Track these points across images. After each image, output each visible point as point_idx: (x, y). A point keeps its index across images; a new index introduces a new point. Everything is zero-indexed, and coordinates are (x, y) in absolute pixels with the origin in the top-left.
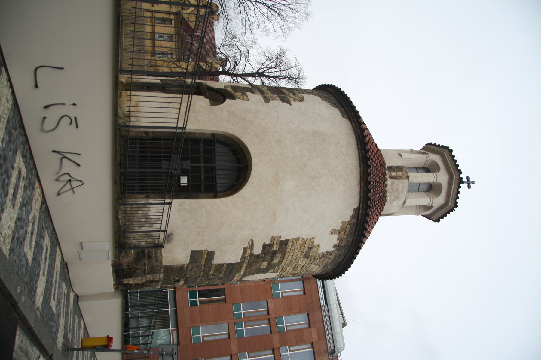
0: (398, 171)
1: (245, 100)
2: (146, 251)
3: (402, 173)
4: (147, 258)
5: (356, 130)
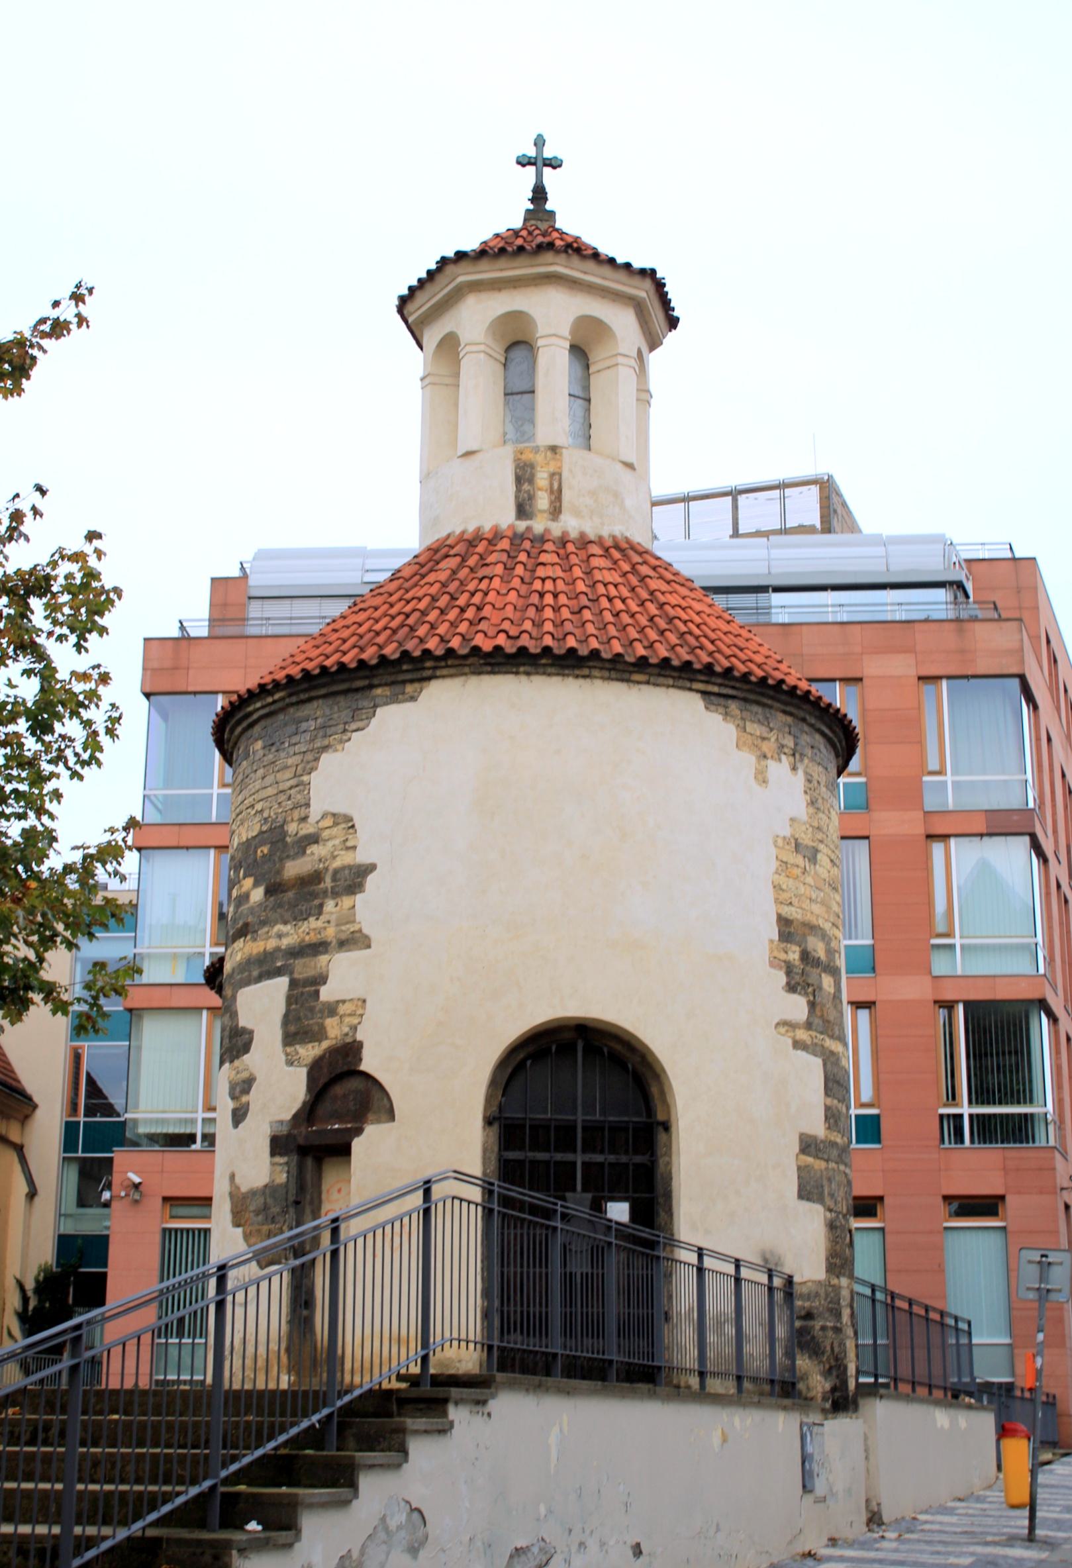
0: (531, 481)
1: (360, 1012)
2: (798, 1324)
3: (539, 469)
4: (811, 1323)
5: (467, 670)
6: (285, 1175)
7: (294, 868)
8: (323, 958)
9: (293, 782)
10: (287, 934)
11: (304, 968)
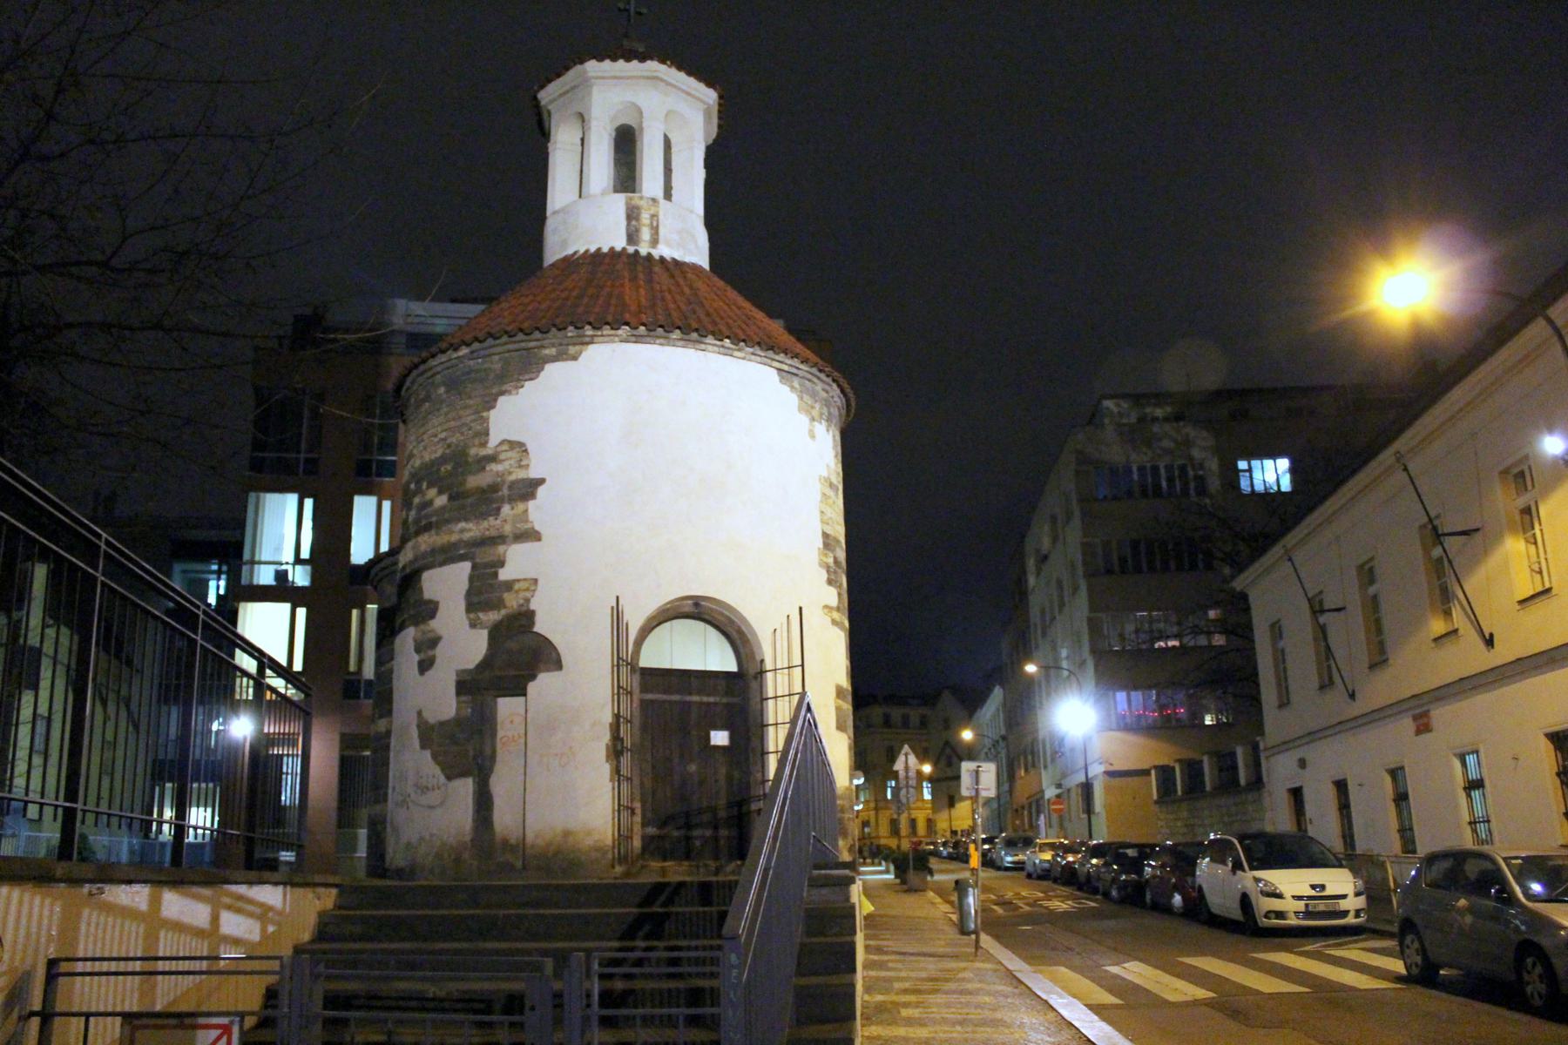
0: (637, 219)
6: (469, 710)
7: (474, 481)
8: (501, 549)
9: (473, 417)
10: (470, 530)
11: (484, 555)
